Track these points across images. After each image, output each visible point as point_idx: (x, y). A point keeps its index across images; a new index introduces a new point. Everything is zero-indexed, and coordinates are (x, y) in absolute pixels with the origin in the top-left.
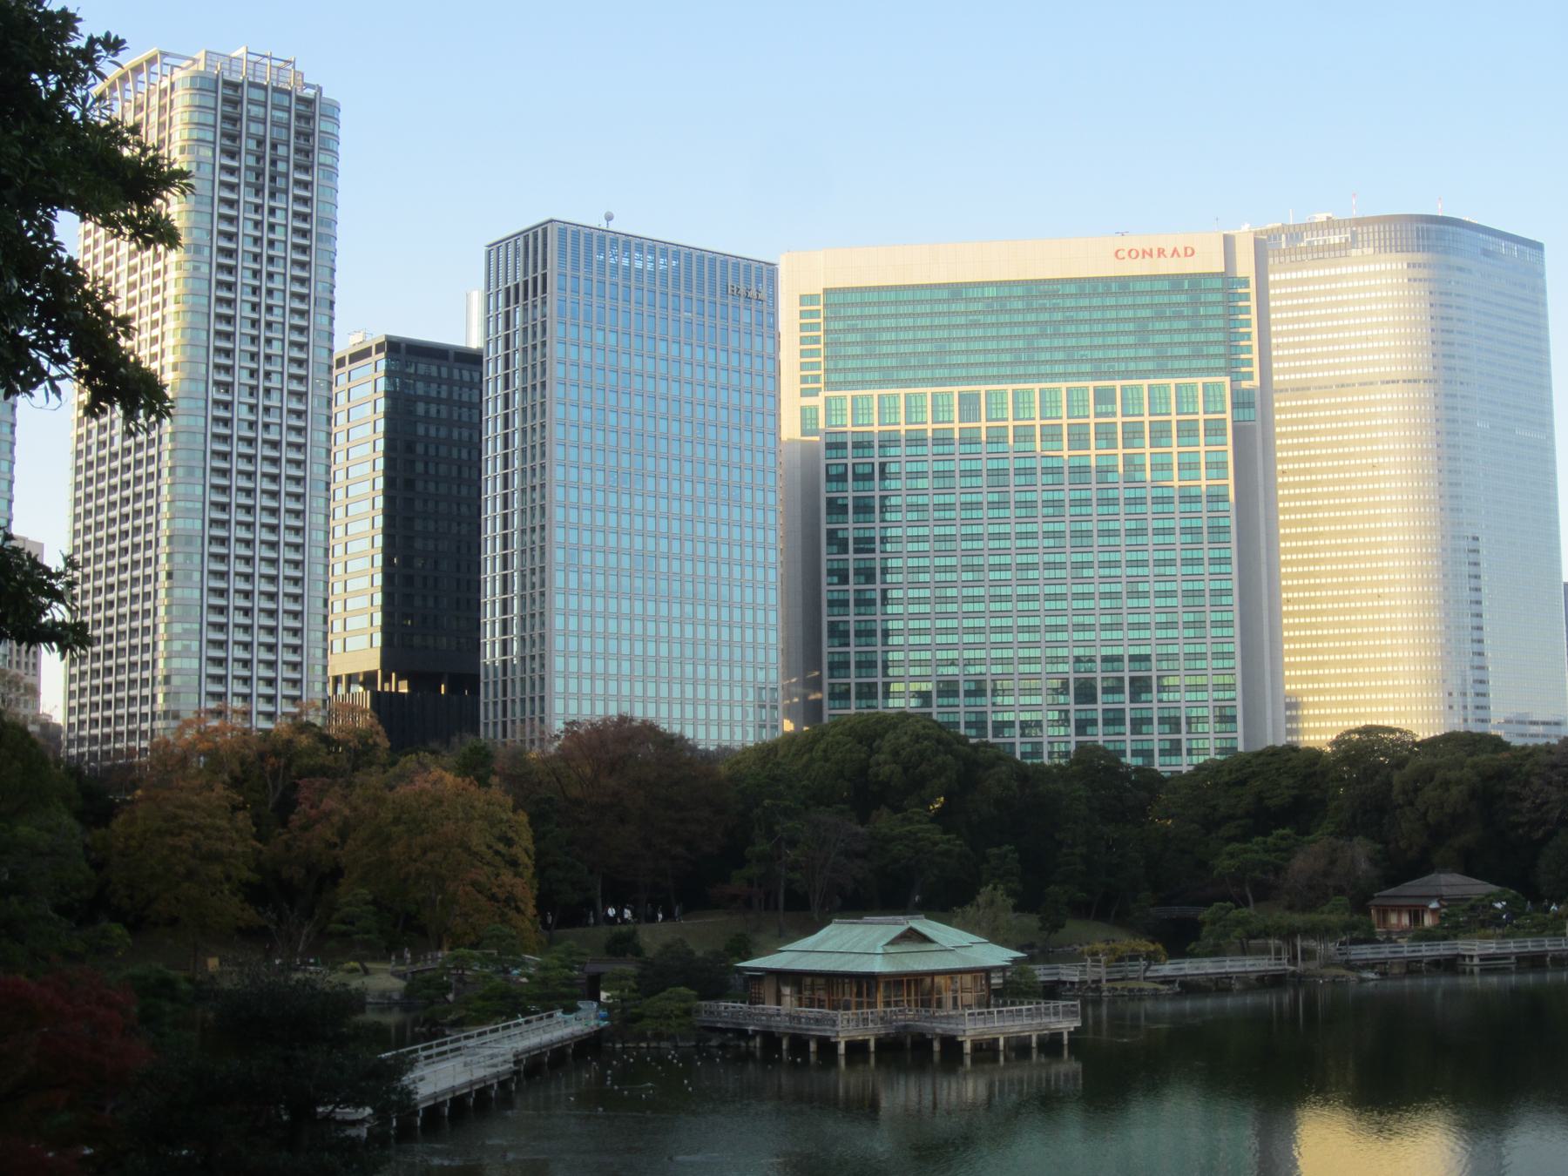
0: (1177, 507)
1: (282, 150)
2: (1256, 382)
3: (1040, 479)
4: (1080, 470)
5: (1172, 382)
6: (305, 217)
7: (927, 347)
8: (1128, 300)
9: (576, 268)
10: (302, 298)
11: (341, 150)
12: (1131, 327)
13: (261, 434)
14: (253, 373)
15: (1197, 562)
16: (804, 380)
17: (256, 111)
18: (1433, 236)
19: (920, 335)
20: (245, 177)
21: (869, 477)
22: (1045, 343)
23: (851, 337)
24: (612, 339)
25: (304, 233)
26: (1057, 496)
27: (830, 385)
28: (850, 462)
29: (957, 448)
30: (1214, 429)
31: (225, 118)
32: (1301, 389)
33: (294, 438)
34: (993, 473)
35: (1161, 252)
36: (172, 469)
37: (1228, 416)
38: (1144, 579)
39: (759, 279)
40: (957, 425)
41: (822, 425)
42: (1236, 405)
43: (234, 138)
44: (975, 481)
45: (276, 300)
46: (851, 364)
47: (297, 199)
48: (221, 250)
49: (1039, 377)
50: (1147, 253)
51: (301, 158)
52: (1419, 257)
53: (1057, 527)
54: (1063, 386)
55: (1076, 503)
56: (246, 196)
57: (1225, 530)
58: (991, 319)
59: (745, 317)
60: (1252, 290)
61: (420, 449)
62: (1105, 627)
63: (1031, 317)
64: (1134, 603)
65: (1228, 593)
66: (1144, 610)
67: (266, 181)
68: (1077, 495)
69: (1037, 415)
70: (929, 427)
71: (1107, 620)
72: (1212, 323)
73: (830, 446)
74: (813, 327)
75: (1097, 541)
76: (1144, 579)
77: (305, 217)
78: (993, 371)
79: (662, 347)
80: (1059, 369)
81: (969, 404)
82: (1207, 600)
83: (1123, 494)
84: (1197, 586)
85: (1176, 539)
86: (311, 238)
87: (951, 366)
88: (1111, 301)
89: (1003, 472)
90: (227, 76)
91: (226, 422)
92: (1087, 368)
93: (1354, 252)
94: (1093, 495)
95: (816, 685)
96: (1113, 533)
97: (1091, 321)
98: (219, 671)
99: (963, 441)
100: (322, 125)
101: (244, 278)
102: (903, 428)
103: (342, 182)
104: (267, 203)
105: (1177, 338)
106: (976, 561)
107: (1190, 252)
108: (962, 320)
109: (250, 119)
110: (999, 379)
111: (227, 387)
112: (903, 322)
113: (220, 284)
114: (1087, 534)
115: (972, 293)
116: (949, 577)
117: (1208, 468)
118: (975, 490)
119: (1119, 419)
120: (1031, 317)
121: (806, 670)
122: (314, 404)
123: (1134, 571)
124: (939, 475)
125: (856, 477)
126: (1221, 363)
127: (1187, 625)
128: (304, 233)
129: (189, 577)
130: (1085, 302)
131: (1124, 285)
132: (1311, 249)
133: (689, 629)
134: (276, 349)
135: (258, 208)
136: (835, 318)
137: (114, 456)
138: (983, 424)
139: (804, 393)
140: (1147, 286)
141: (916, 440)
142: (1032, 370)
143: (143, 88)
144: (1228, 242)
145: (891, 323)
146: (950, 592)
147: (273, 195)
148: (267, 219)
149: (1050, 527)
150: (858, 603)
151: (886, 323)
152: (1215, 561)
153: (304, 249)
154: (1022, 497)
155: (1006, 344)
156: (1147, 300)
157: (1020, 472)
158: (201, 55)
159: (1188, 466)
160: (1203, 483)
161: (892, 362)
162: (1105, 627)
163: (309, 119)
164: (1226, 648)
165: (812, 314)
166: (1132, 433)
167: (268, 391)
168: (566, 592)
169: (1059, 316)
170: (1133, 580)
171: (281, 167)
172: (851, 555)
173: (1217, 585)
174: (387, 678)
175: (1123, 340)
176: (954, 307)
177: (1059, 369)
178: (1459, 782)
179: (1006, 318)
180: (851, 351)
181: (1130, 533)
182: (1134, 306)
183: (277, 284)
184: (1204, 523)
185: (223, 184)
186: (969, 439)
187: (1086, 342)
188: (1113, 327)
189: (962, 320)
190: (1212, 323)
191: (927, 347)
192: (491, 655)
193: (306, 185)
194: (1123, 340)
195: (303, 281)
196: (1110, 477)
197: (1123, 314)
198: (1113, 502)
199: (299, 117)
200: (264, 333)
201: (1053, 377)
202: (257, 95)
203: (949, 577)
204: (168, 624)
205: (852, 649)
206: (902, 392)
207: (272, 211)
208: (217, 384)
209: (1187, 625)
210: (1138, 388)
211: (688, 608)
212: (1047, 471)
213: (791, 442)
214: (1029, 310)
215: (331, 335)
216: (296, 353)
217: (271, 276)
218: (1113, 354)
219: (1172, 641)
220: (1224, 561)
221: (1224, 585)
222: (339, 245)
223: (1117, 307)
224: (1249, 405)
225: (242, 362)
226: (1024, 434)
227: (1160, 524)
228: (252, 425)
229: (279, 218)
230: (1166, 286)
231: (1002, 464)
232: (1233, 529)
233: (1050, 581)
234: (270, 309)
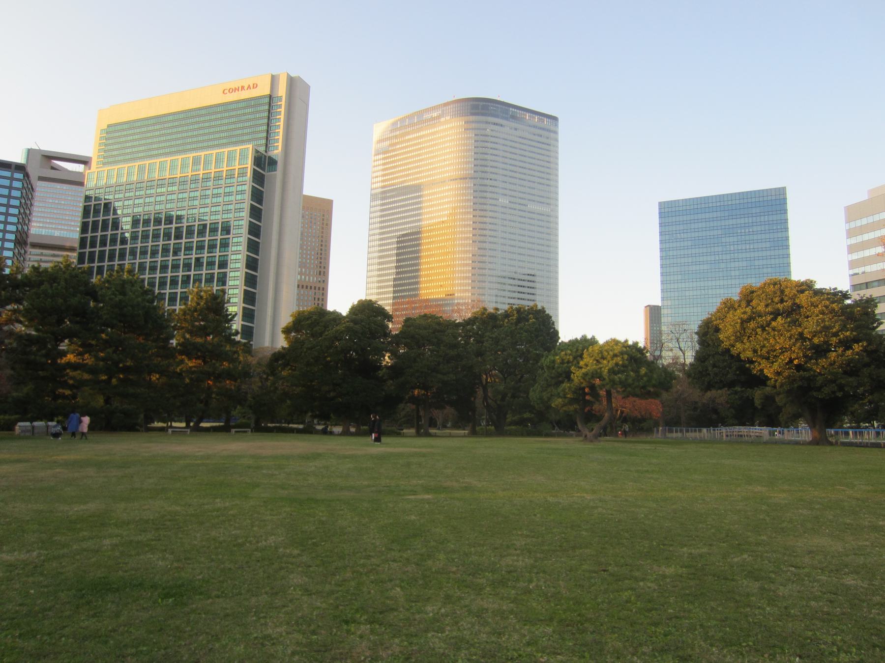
50: (236, 90)
60: (283, 103)
81: (141, 169)
93: (442, 119)
107: (255, 86)
144: (274, 79)
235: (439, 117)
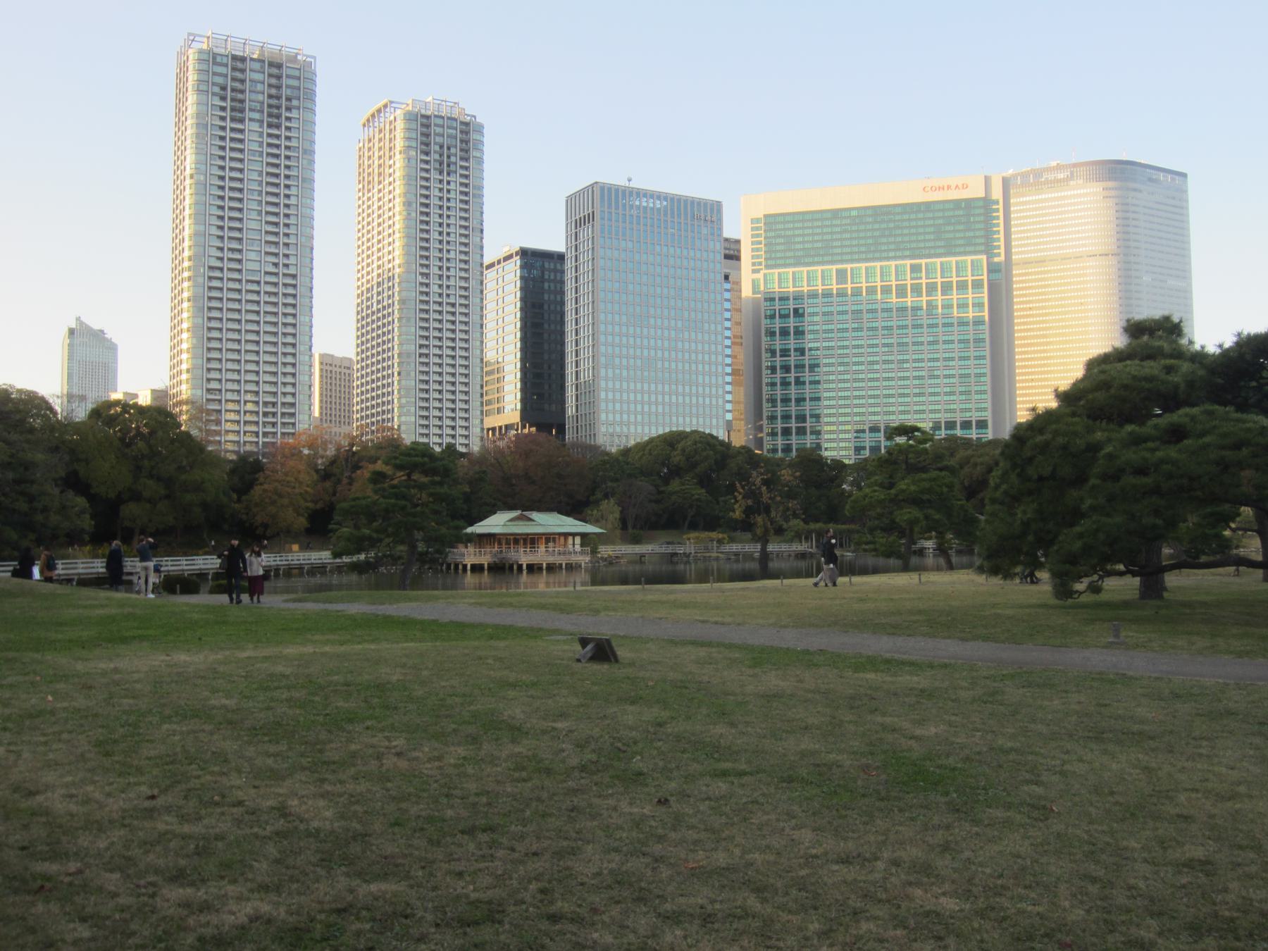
0: (955, 328)
1: (453, 150)
2: (1002, 258)
3: (880, 315)
4: (902, 310)
5: (953, 259)
6: (466, 185)
7: (819, 245)
8: (931, 215)
9: (610, 206)
10: (466, 228)
11: (485, 149)
12: (932, 229)
13: (445, 300)
14: (440, 268)
15: (968, 358)
16: (754, 264)
17: (439, 130)
18: (1120, 173)
19: (816, 238)
20: (433, 165)
21: (788, 316)
22: (884, 240)
23: (778, 240)
24: (630, 245)
25: (466, 194)
26: (889, 324)
27: (767, 267)
28: (777, 308)
29: (834, 299)
30: (977, 285)
31: (422, 134)
32: (1027, 263)
33: (463, 301)
34: (854, 312)
35: (949, 187)
36: (399, 319)
37: (985, 277)
38: (938, 368)
39: (712, 210)
40: (835, 287)
41: (762, 288)
42: (990, 271)
43: (427, 145)
44: (845, 317)
45: (452, 230)
46: (778, 255)
47: (461, 175)
48: (422, 204)
49: (880, 259)
50: (941, 188)
51: (463, 154)
52: (1111, 184)
53: (890, 341)
54: (893, 263)
55: (899, 327)
56: (434, 175)
57: (983, 340)
58: (854, 228)
59: (705, 231)
60: (1001, 206)
61: (546, 307)
62: (916, 395)
63: (877, 226)
64: (932, 381)
65: (984, 375)
66: (937, 385)
67: (445, 167)
68: (900, 323)
69: (878, 279)
70: (820, 288)
71: (917, 391)
72: (978, 226)
73: (766, 300)
74: (758, 236)
75: (911, 348)
76: (938, 368)
77: (466, 185)
78: (856, 257)
79: (658, 248)
80: (892, 254)
81: (841, 275)
82: (973, 379)
83: (925, 322)
84: (967, 372)
85: (955, 346)
86: (470, 196)
87: (832, 255)
88: (921, 216)
89: (860, 311)
90: (423, 112)
91: (427, 294)
92: (908, 253)
93: (1072, 183)
94: (909, 323)
95: (760, 429)
96: (922, 343)
97: (910, 227)
98: (426, 422)
99: (839, 295)
100: (473, 136)
101: (434, 218)
102: (805, 289)
103: (486, 166)
104: (446, 178)
105: (958, 235)
106: (846, 360)
107: (965, 186)
108: (838, 229)
109: (436, 134)
110: (859, 261)
111: (427, 275)
112: (806, 231)
113: (422, 222)
114: (906, 344)
115: (847, 214)
116: (831, 369)
117: (975, 306)
118: (846, 322)
119: (924, 281)
120: (877, 226)
121: (755, 422)
122: (473, 283)
123: (931, 364)
124: (825, 314)
125: (781, 316)
126: (982, 248)
127: (961, 393)
128: (466, 194)
129: (409, 374)
130: (906, 217)
131: (928, 206)
132: (1047, 182)
133: (674, 398)
134: (452, 255)
135: (441, 181)
136: (771, 230)
137: (373, 313)
138: (849, 286)
139: (754, 271)
140: (941, 207)
141: (813, 295)
142: (877, 255)
143: (382, 120)
144: (987, 180)
145: (800, 232)
146: (832, 377)
147: (449, 174)
148: (446, 187)
149: (886, 341)
150: (782, 384)
151: (797, 232)
152: (976, 358)
153: (466, 202)
154: (870, 325)
155: (862, 242)
156: (941, 214)
157: (869, 311)
158: (410, 102)
159: (963, 306)
160: (971, 315)
161: (800, 253)
162: (916, 395)
163: (467, 133)
164: (983, 405)
165: (757, 229)
166: (931, 288)
167: (448, 277)
168: (607, 379)
169: (892, 225)
170: (931, 369)
171: (453, 159)
172: (778, 359)
173: (978, 371)
174: (524, 427)
175: (927, 237)
176: (835, 222)
177: (892, 254)
178: (982, 464)
179: (862, 227)
180: (778, 248)
181: (930, 343)
182: (934, 218)
183: (452, 221)
184: (971, 337)
185: (422, 169)
186: (842, 294)
187: (906, 239)
188: (921, 230)
189: (838, 229)
190: (978, 226)
191: (819, 245)
192: (570, 410)
193: (467, 168)
194: (927, 237)
195: (466, 219)
196: (919, 313)
197: (928, 222)
198: (921, 326)
199: (462, 132)
200: (445, 247)
201: (888, 259)
202: (440, 121)
203: (831, 369)
204: (399, 399)
205: (779, 409)
206: (805, 269)
207: (448, 183)
208: (422, 274)
209: (961, 393)
210: (935, 263)
211: (674, 387)
212: (884, 310)
213: (747, 298)
214: (876, 222)
215: (482, 248)
216: (463, 257)
217: (448, 217)
218: (922, 245)
219: (953, 402)
220: (983, 357)
221: (982, 371)
222: (485, 199)
223: (924, 219)
224: (999, 271)
225: (434, 262)
226: (872, 291)
227: (946, 338)
228: (440, 295)
229: (452, 186)
230: (951, 206)
231: (859, 307)
232: (988, 340)
233: (885, 371)
234: (448, 234)
235: (1067, 180)
